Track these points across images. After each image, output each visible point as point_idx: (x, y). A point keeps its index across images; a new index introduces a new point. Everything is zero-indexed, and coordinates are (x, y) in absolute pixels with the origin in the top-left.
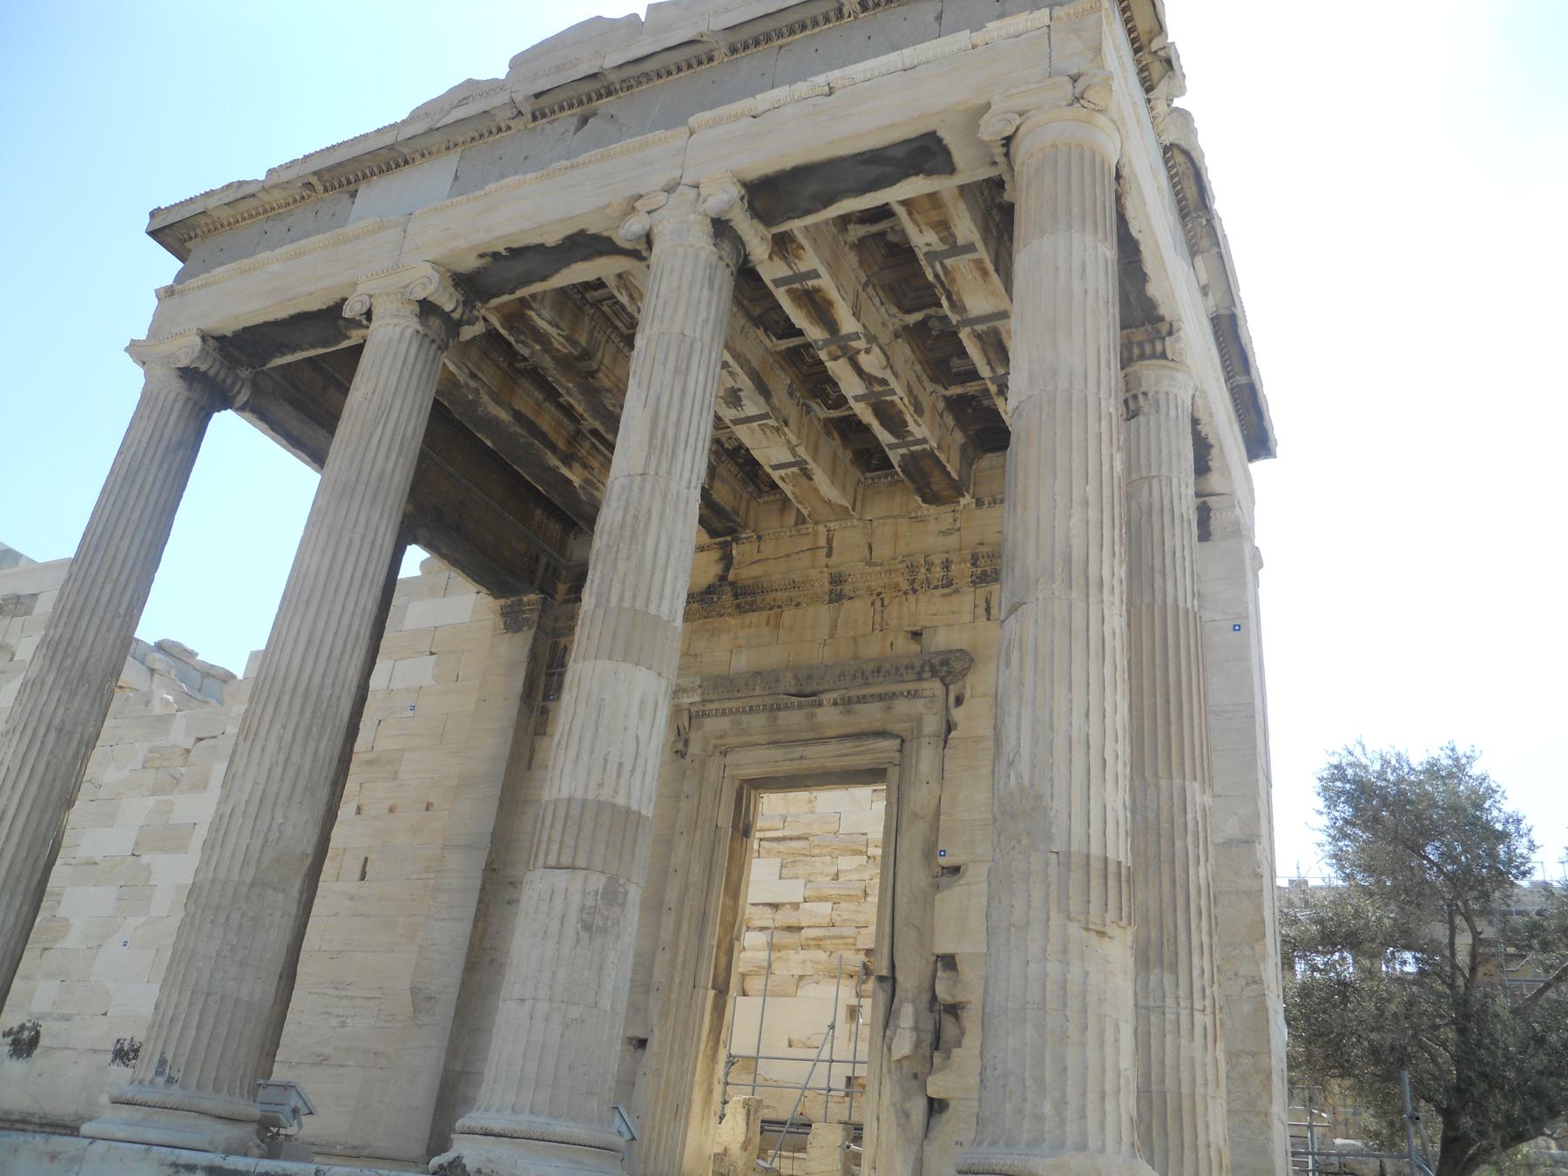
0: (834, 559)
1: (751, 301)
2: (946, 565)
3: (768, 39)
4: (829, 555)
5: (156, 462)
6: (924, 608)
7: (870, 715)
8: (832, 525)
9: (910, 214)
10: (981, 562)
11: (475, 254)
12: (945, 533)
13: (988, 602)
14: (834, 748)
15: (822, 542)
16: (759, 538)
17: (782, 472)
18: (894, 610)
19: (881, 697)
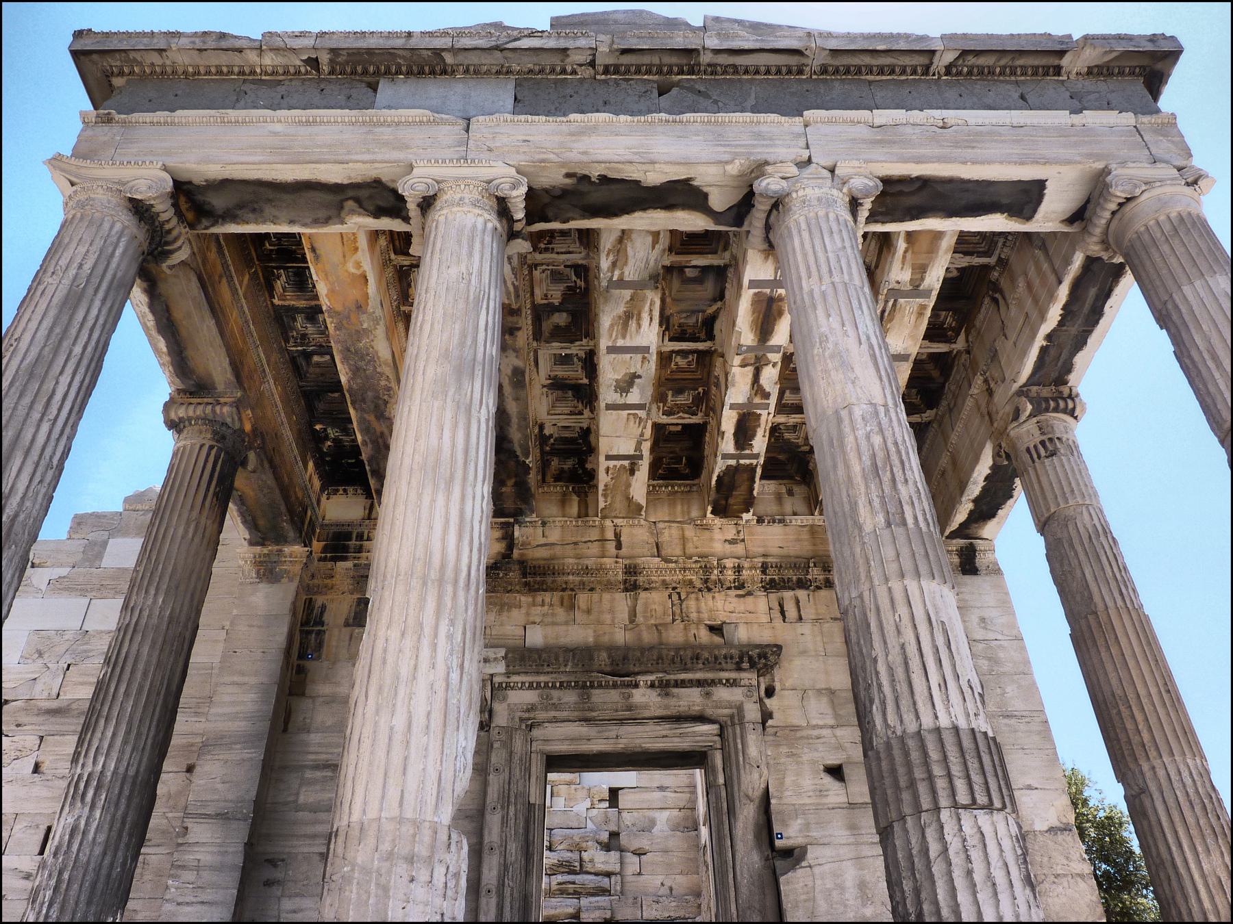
0: (624, 551)
1: (674, 300)
2: (738, 569)
3: (859, 72)
4: (619, 546)
5: (101, 294)
6: (722, 606)
7: (690, 699)
8: (618, 521)
9: (905, 252)
10: (770, 571)
11: (564, 171)
12: (732, 542)
13: (781, 606)
14: (652, 729)
15: (610, 535)
16: (544, 524)
17: (612, 463)
18: (691, 604)
19: (700, 683)
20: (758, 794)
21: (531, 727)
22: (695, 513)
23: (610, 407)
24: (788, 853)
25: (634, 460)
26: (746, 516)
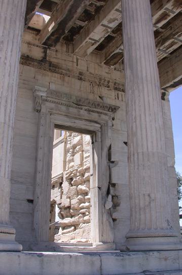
0: (79, 67)
2: (109, 82)
4: (77, 65)
6: (104, 91)
7: (95, 116)
8: (78, 57)
10: (116, 85)
12: (107, 73)
14: (84, 122)
15: (75, 61)
16: (56, 51)
19: (98, 112)
20: (108, 146)
21: (51, 114)
22: (98, 61)
23: (102, 25)
24: (113, 162)
25: (96, 41)
26: (112, 67)
